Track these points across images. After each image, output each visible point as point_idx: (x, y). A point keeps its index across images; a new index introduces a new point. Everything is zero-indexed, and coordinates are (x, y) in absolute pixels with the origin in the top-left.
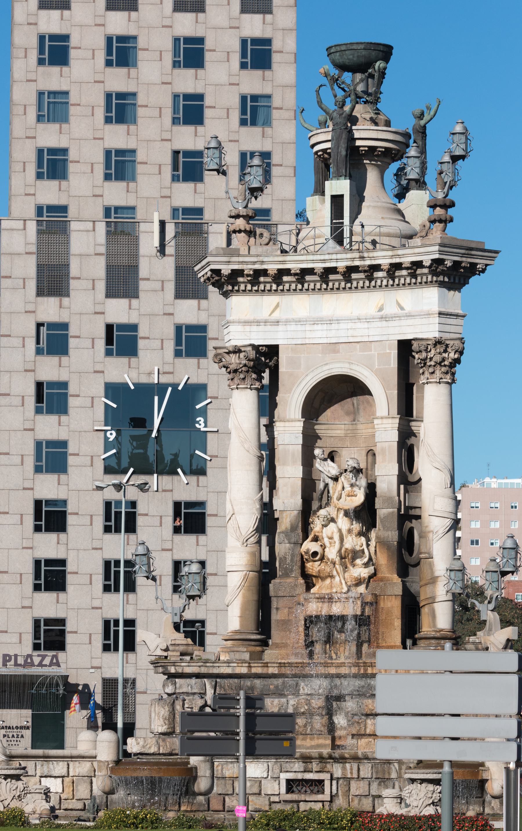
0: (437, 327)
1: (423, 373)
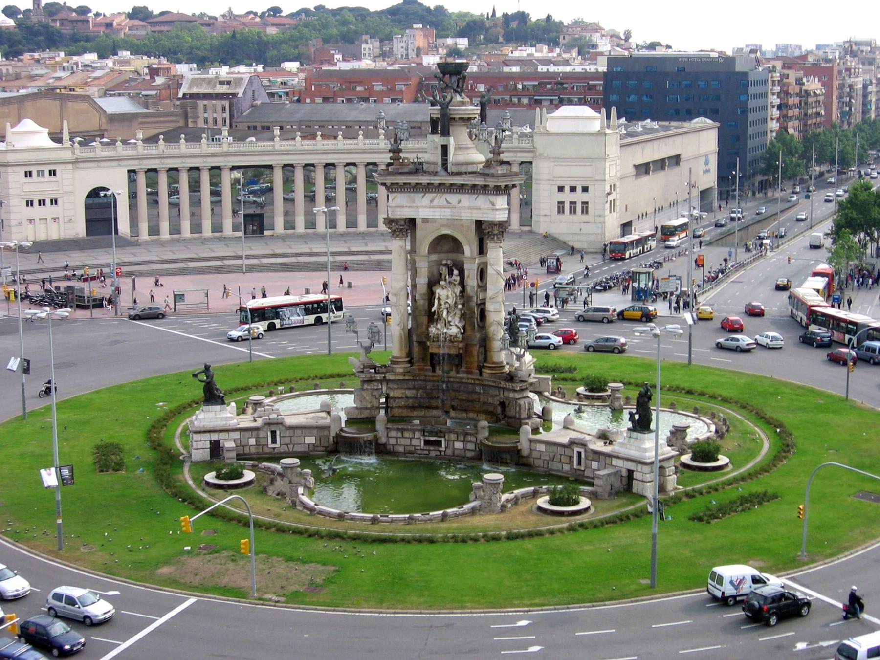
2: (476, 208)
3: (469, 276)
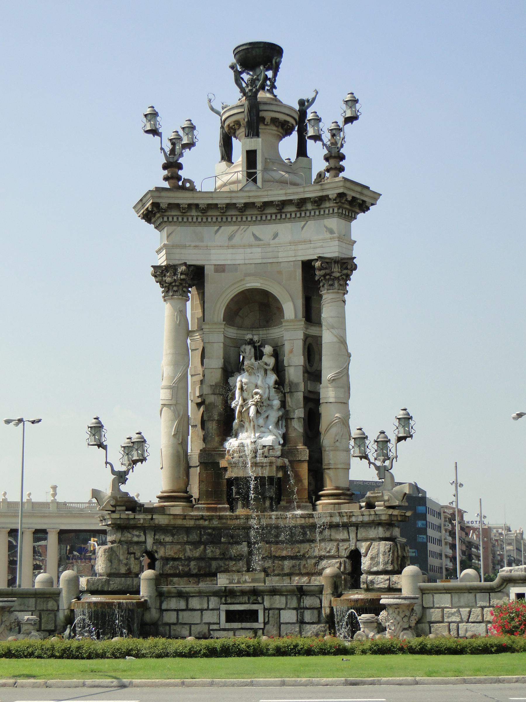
0: (336, 249)
1: (323, 286)
2: (304, 242)
3: (291, 352)
